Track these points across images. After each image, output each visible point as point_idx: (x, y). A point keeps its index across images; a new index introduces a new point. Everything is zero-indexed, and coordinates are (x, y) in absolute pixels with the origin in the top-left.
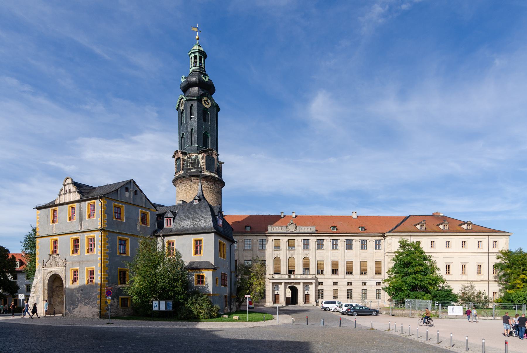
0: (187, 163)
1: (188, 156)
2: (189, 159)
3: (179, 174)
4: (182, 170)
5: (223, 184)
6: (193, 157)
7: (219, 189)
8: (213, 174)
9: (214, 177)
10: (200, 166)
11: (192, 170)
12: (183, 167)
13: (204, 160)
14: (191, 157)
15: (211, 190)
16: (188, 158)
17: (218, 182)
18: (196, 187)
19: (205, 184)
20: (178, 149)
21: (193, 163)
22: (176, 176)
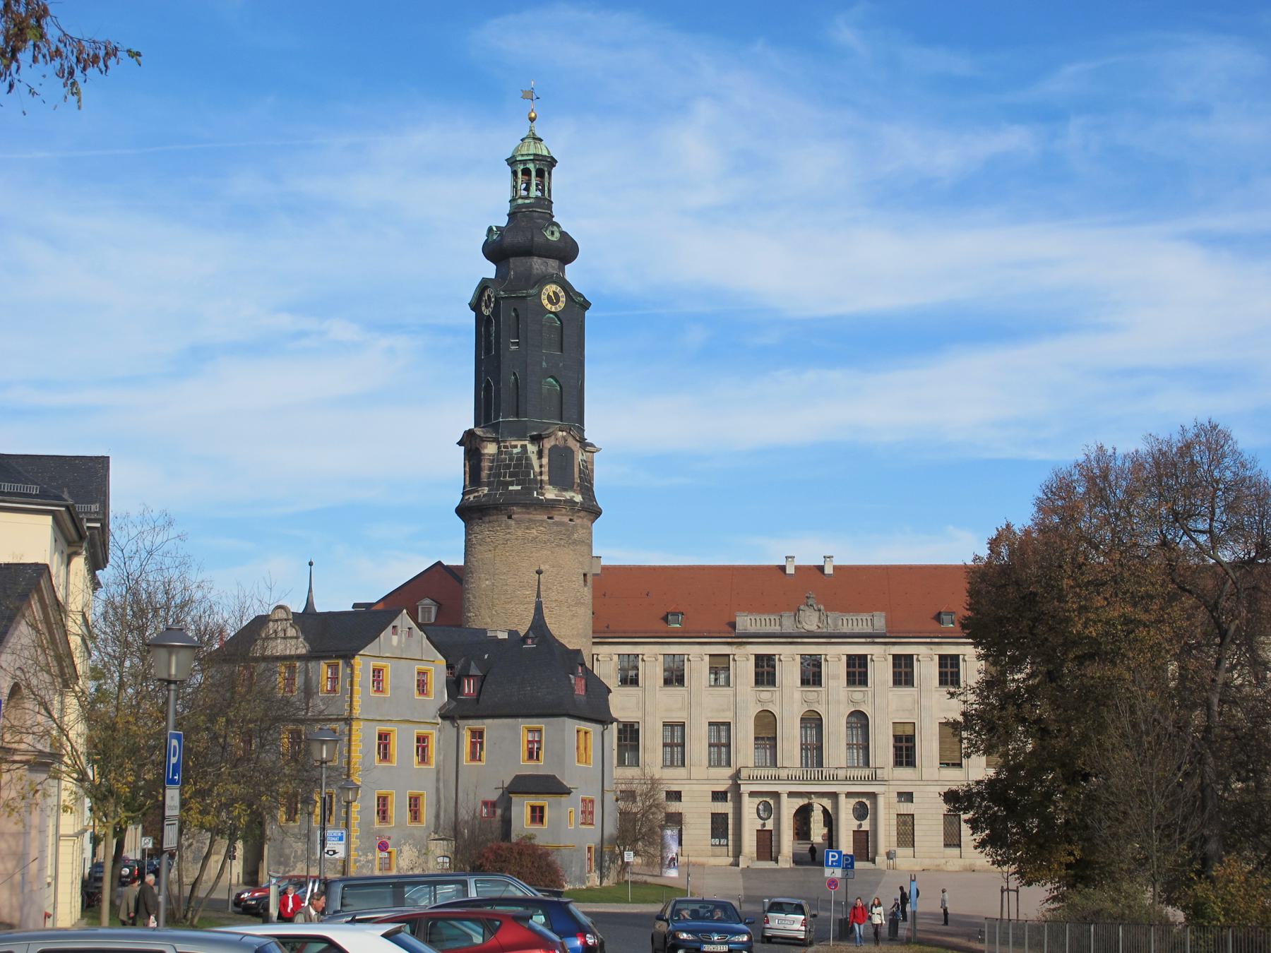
0: (499, 467)
1: (499, 448)
2: (503, 456)
3: (476, 494)
4: (489, 484)
5: (595, 513)
6: (515, 451)
7: (585, 531)
8: (568, 495)
9: (571, 502)
10: (532, 476)
11: (511, 488)
12: (489, 476)
13: (545, 461)
14: (510, 449)
15: (561, 539)
16: (500, 452)
17: (582, 514)
18: (520, 533)
19: (544, 524)
20: (473, 427)
21: (516, 466)
22: (467, 497)
